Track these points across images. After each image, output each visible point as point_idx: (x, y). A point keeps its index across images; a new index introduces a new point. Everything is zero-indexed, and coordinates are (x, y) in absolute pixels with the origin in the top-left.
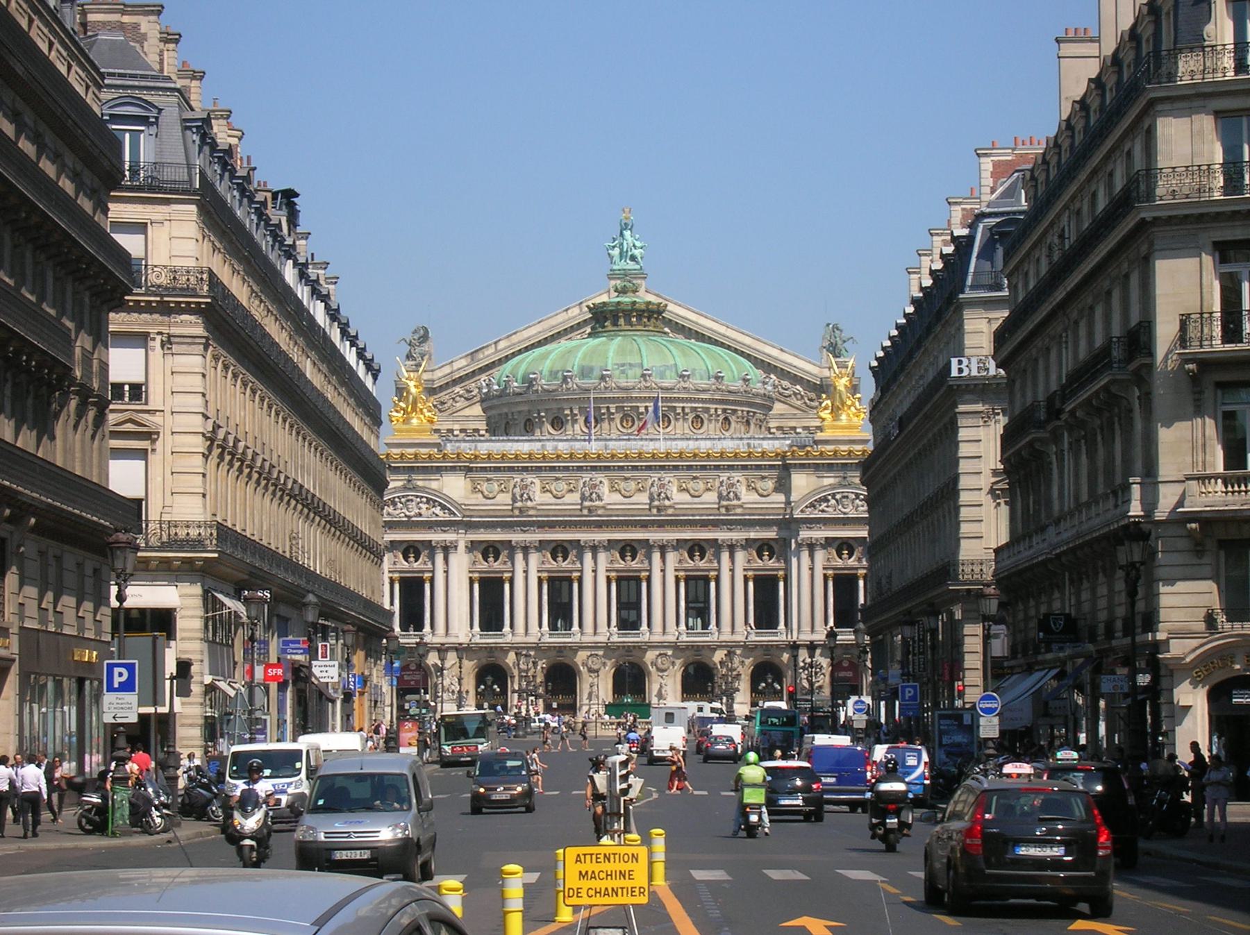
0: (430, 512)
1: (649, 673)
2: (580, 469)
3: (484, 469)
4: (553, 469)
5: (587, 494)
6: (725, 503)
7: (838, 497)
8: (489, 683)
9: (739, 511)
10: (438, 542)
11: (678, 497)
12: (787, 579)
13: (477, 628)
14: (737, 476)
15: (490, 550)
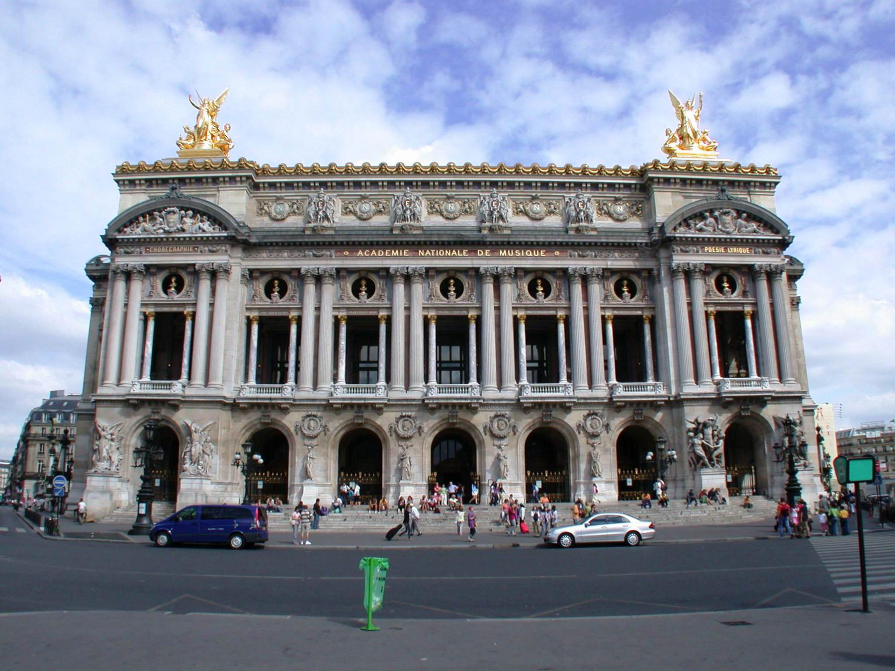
0: (197, 226)
1: (482, 442)
2: (391, 184)
3: (272, 185)
4: (357, 185)
5: (400, 212)
6: (574, 225)
7: (717, 213)
8: (249, 450)
9: (595, 233)
10: (203, 266)
11: (516, 221)
12: (653, 321)
13: (252, 381)
14: (586, 195)
15: (277, 282)
